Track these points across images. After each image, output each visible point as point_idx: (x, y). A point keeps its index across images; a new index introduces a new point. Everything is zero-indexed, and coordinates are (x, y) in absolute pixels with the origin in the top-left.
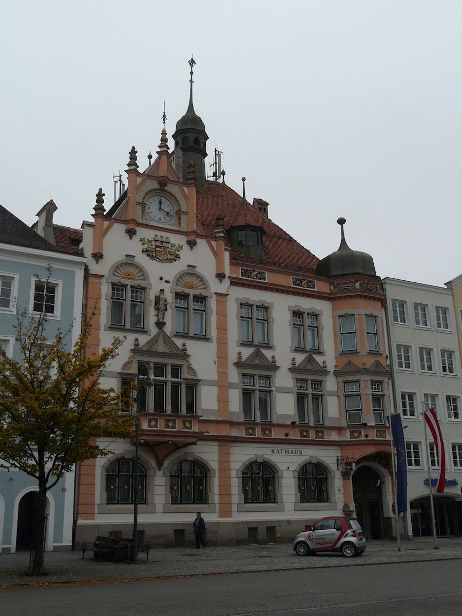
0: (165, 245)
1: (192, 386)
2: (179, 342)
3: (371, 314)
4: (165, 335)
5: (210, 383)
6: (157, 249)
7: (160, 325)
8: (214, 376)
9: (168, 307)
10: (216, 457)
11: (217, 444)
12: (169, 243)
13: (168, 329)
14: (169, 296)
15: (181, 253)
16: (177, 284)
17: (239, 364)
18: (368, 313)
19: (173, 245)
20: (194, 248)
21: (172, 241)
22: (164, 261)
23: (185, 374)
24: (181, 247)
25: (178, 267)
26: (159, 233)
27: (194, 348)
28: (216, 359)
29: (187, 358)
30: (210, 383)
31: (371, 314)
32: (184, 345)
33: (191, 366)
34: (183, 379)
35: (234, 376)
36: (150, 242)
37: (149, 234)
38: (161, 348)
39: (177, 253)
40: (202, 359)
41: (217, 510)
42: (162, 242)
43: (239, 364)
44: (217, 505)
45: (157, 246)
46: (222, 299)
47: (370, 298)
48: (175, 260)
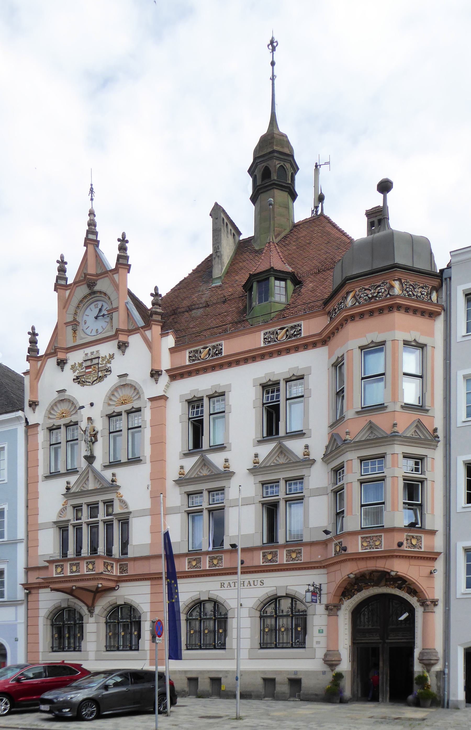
0: (95, 361)
1: (125, 522)
2: (107, 474)
3: (415, 340)
4: (95, 472)
5: (142, 513)
6: (87, 371)
7: (90, 459)
8: (147, 504)
9: (99, 436)
10: (148, 598)
11: (148, 583)
12: (99, 358)
13: (98, 465)
14: (100, 425)
15: (114, 365)
16: (109, 405)
17: (180, 482)
18: (409, 338)
19: (104, 359)
20: (128, 351)
21: (102, 354)
22: (95, 382)
23: (117, 509)
24: (112, 357)
25: (111, 381)
26: (88, 350)
27: (124, 476)
28: (149, 483)
29: (118, 490)
30: (142, 513)
31: (415, 340)
32: (114, 475)
33: (123, 498)
34: (115, 515)
35: (175, 497)
36: (81, 365)
37: (76, 358)
38: (91, 485)
39: (109, 365)
40: (133, 487)
41: (148, 657)
42: (91, 360)
43: (180, 482)
44: (148, 652)
45: (87, 367)
46: (161, 402)
47: (415, 311)
48: (106, 376)
